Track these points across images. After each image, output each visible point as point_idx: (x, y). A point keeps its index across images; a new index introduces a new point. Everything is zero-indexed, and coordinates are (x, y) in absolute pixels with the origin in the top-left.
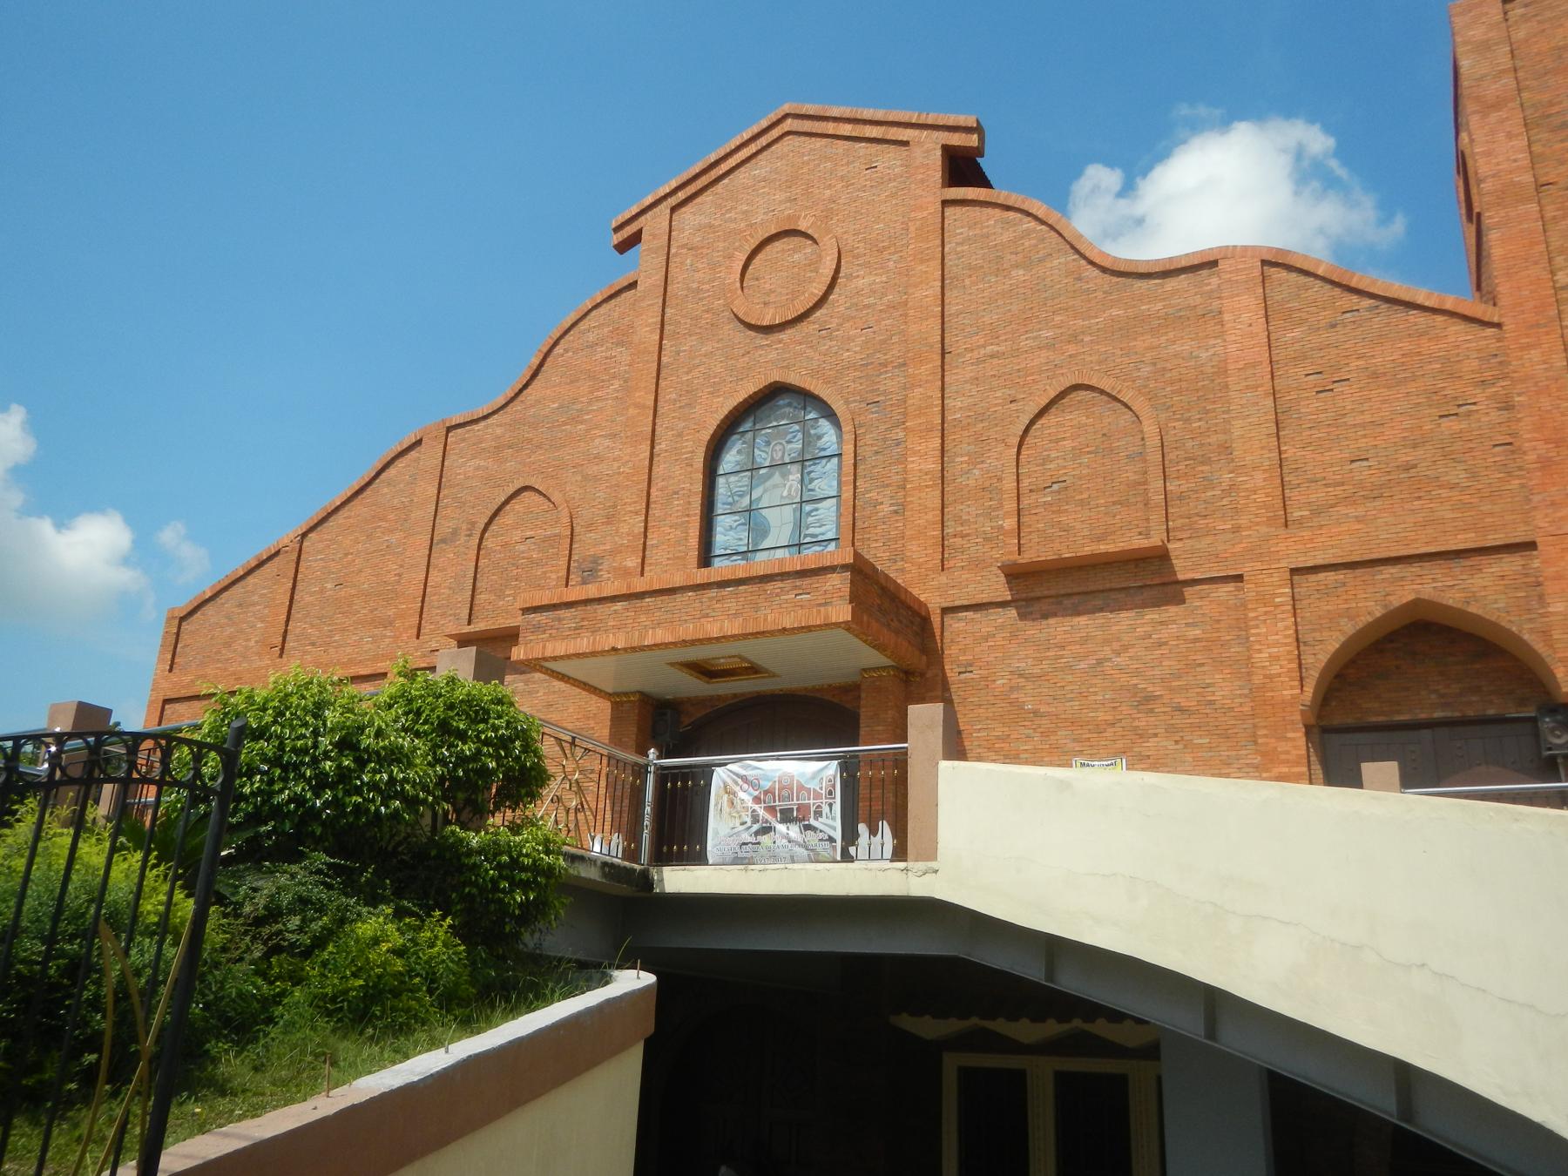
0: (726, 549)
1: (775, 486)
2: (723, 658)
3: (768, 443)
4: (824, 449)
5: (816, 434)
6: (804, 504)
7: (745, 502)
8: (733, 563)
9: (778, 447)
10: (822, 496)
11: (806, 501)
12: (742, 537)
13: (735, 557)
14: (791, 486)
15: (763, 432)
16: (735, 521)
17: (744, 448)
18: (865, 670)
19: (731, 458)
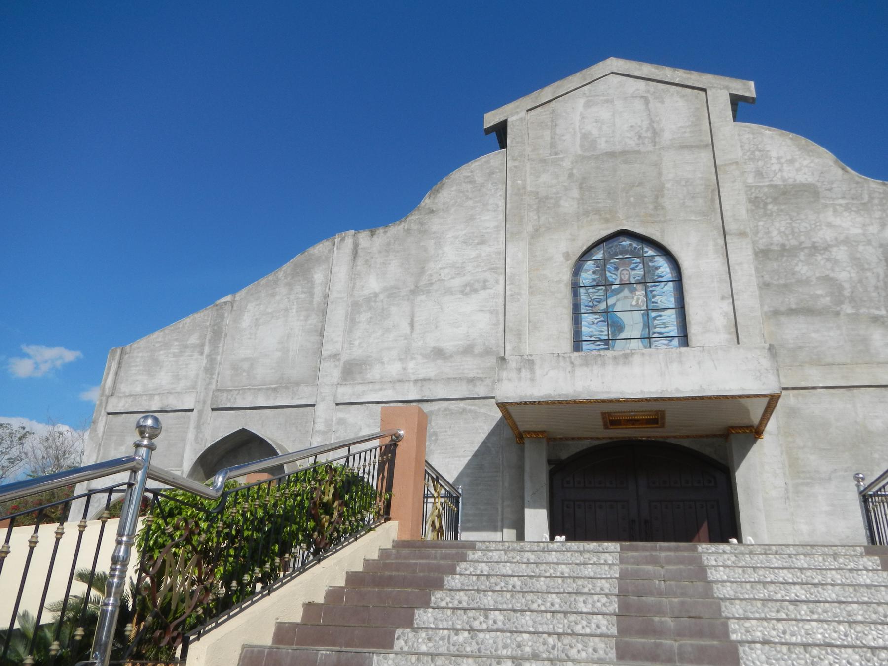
0: (591, 337)
1: (626, 298)
2: (632, 412)
3: (617, 269)
4: (662, 277)
5: (653, 266)
6: (650, 311)
7: (603, 306)
8: (597, 348)
9: (625, 272)
10: (663, 307)
11: (650, 310)
12: (603, 329)
13: (598, 343)
14: (638, 299)
15: (612, 261)
16: (596, 319)
17: (597, 270)
18: (733, 428)
19: (587, 277)
